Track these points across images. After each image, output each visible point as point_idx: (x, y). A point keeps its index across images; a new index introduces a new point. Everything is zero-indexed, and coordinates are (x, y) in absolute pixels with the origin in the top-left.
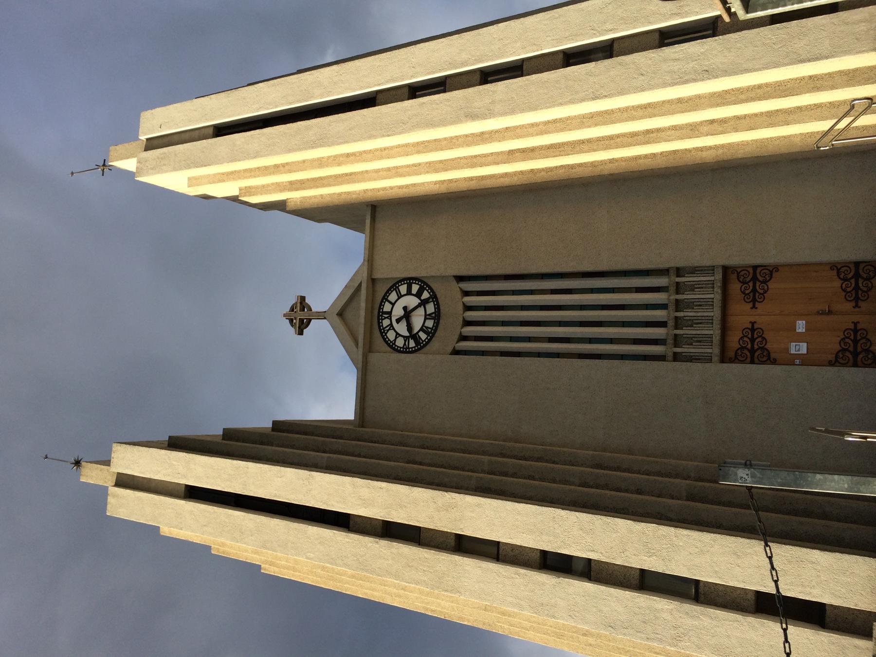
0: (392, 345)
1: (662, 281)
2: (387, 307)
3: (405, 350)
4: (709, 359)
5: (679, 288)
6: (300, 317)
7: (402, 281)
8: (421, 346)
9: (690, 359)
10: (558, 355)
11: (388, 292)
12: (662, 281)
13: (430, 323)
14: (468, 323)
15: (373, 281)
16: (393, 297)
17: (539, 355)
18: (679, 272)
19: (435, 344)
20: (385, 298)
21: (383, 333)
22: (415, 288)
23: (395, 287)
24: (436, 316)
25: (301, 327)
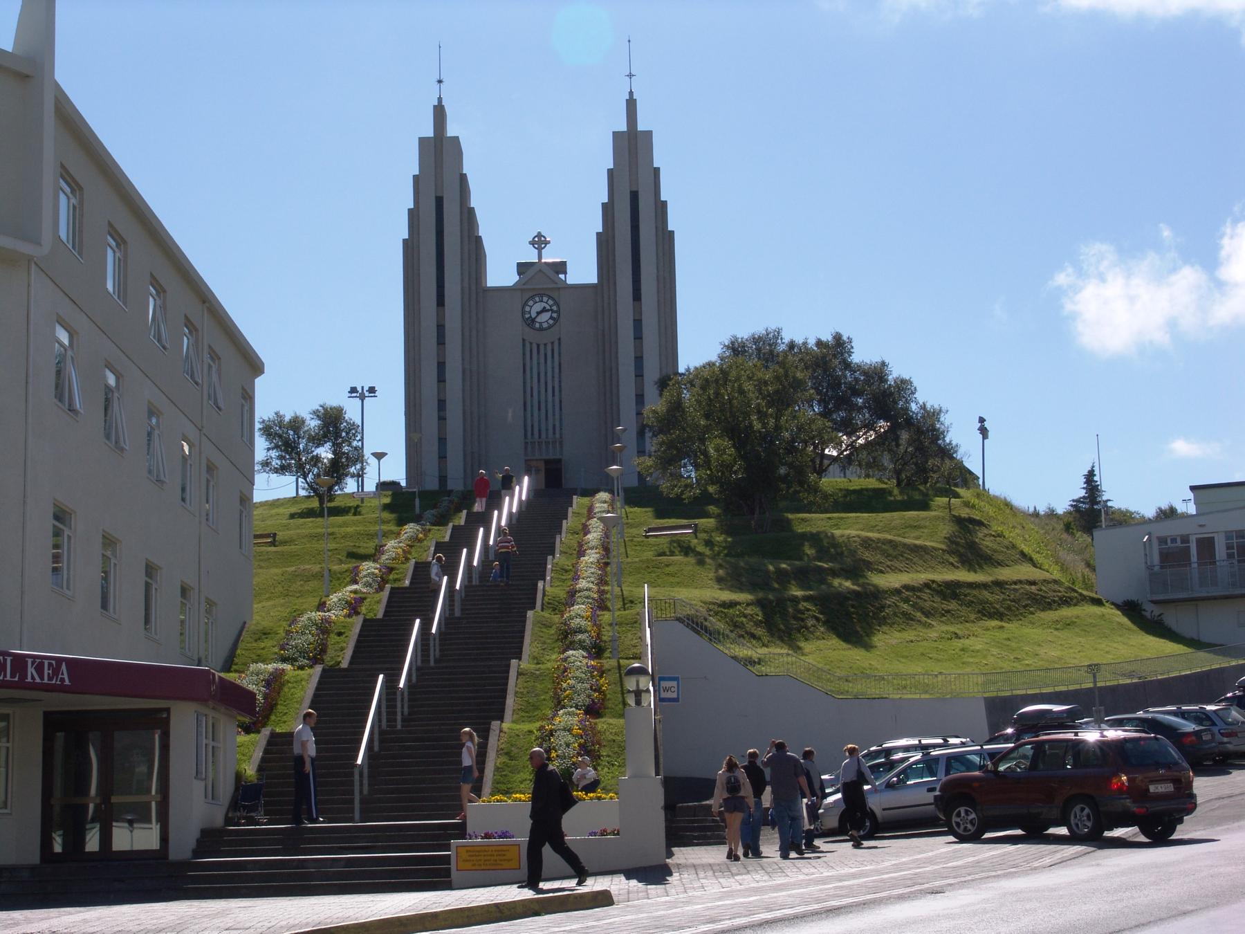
0: (525, 304)
1: (558, 436)
2: (545, 299)
3: (523, 313)
4: (526, 454)
5: (554, 442)
6: (539, 242)
7: (558, 306)
8: (525, 320)
9: (526, 448)
10: (525, 392)
11: (553, 299)
12: (558, 436)
13: (537, 325)
14: (538, 346)
15: (559, 289)
16: (551, 302)
17: (524, 383)
18: (561, 443)
19: (527, 329)
20: (550, 297)
21: (532, 298)
22: (555, 315)
23: (556, 303)
24: (541, 329)
25: (532, 243)
